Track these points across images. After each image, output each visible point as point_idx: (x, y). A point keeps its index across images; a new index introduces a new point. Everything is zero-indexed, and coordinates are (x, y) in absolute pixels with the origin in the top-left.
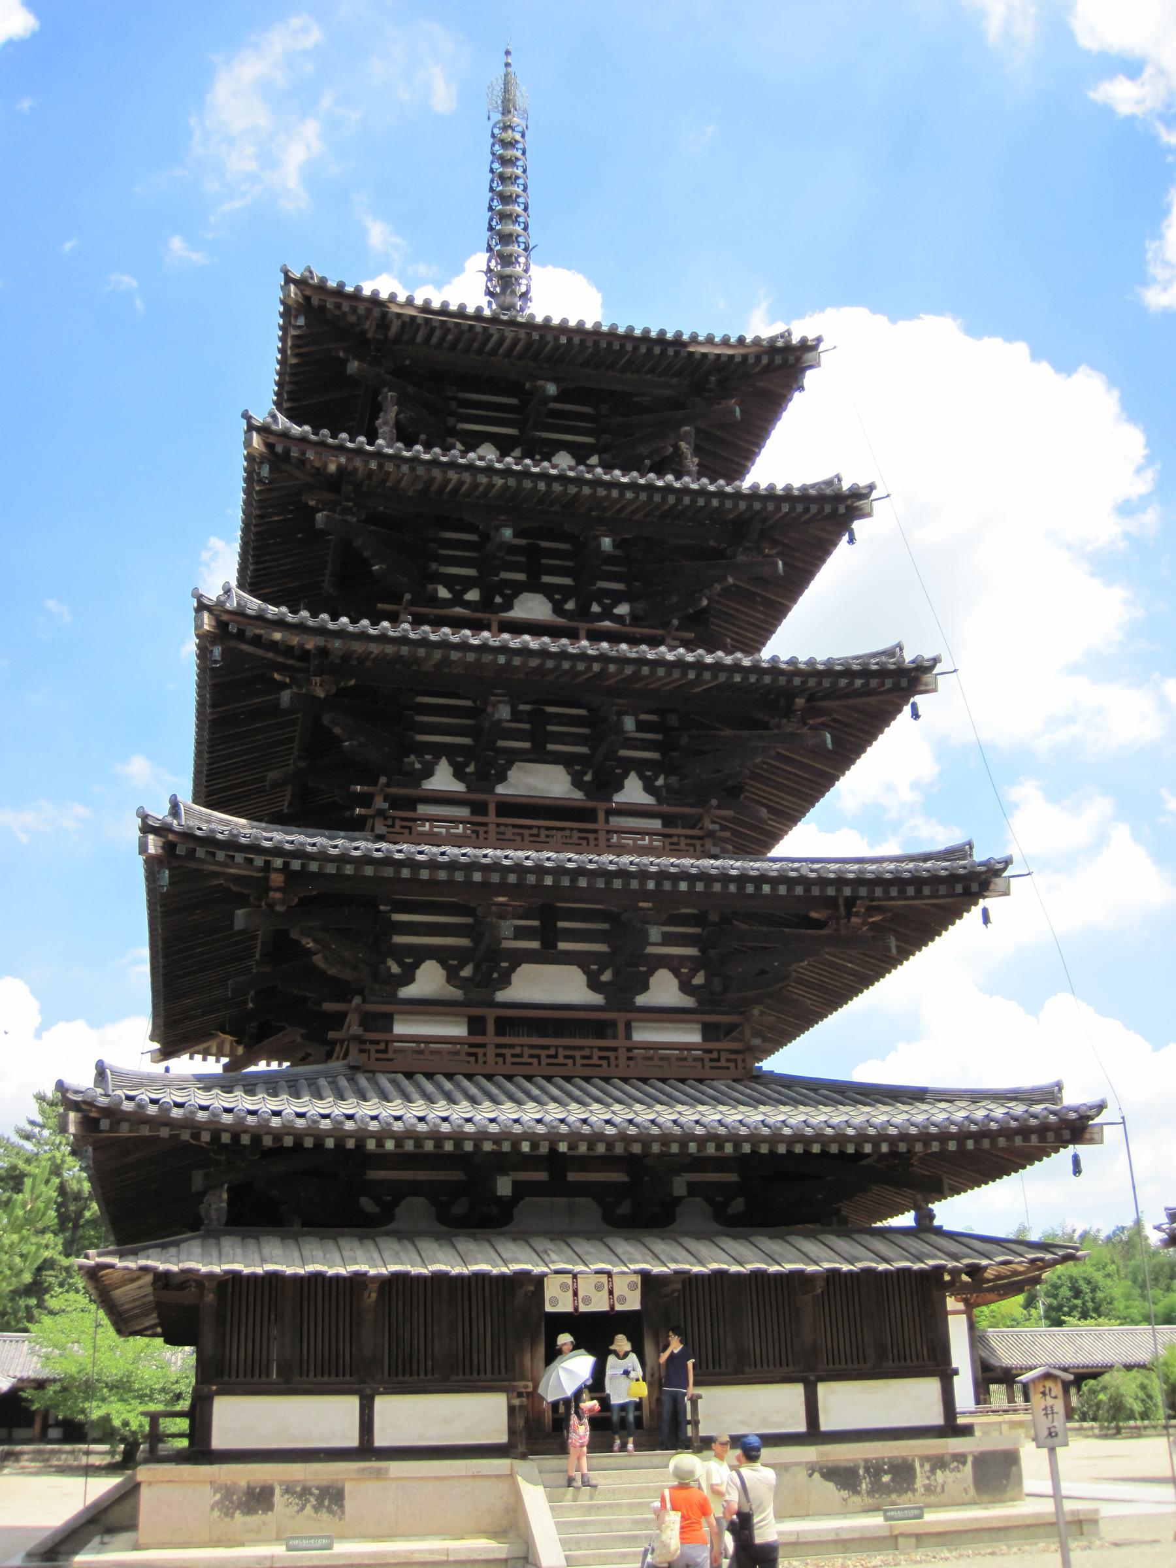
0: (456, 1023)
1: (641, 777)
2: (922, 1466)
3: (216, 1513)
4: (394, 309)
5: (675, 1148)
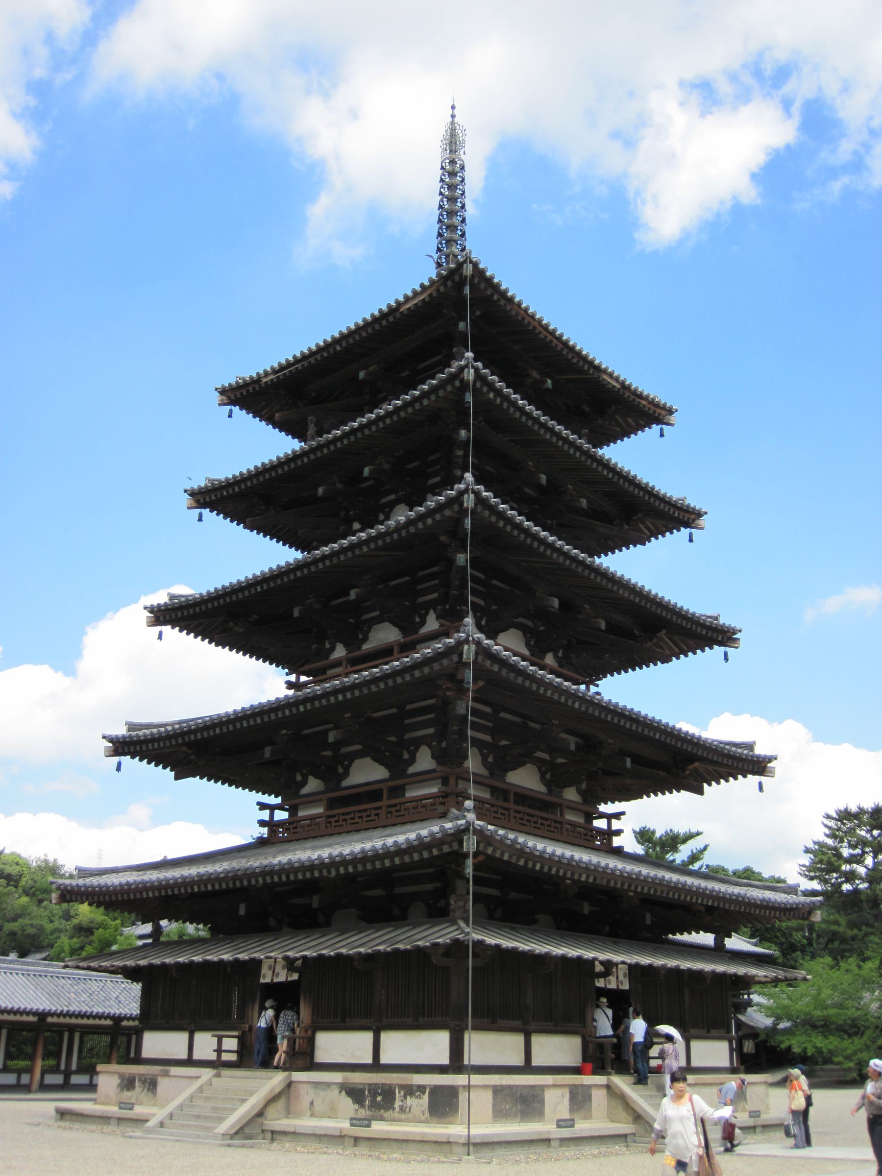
0: (319, 806)
2: (399, 1092)
4: (264, 380)
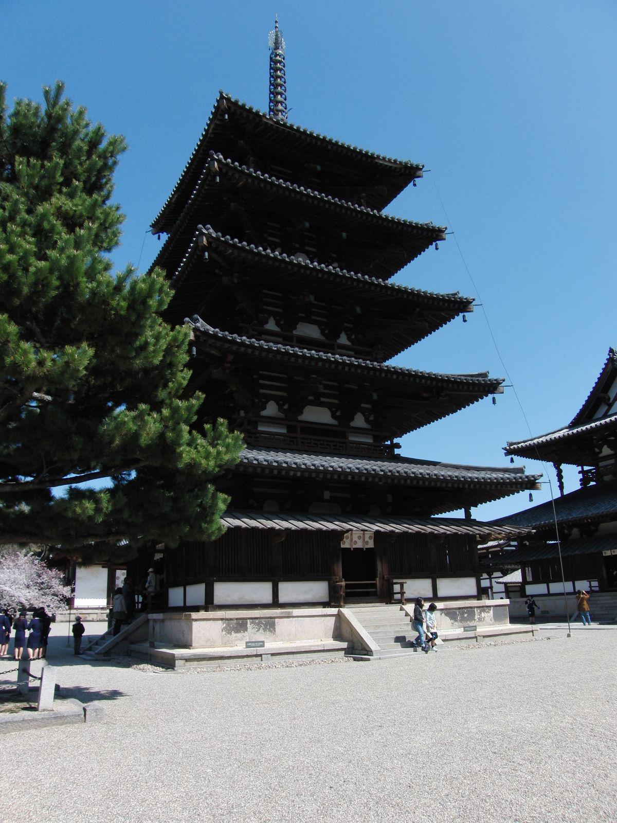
1: (347, 334)
2: (477, 611)
3: (224, 633)
5: (402, 482)
